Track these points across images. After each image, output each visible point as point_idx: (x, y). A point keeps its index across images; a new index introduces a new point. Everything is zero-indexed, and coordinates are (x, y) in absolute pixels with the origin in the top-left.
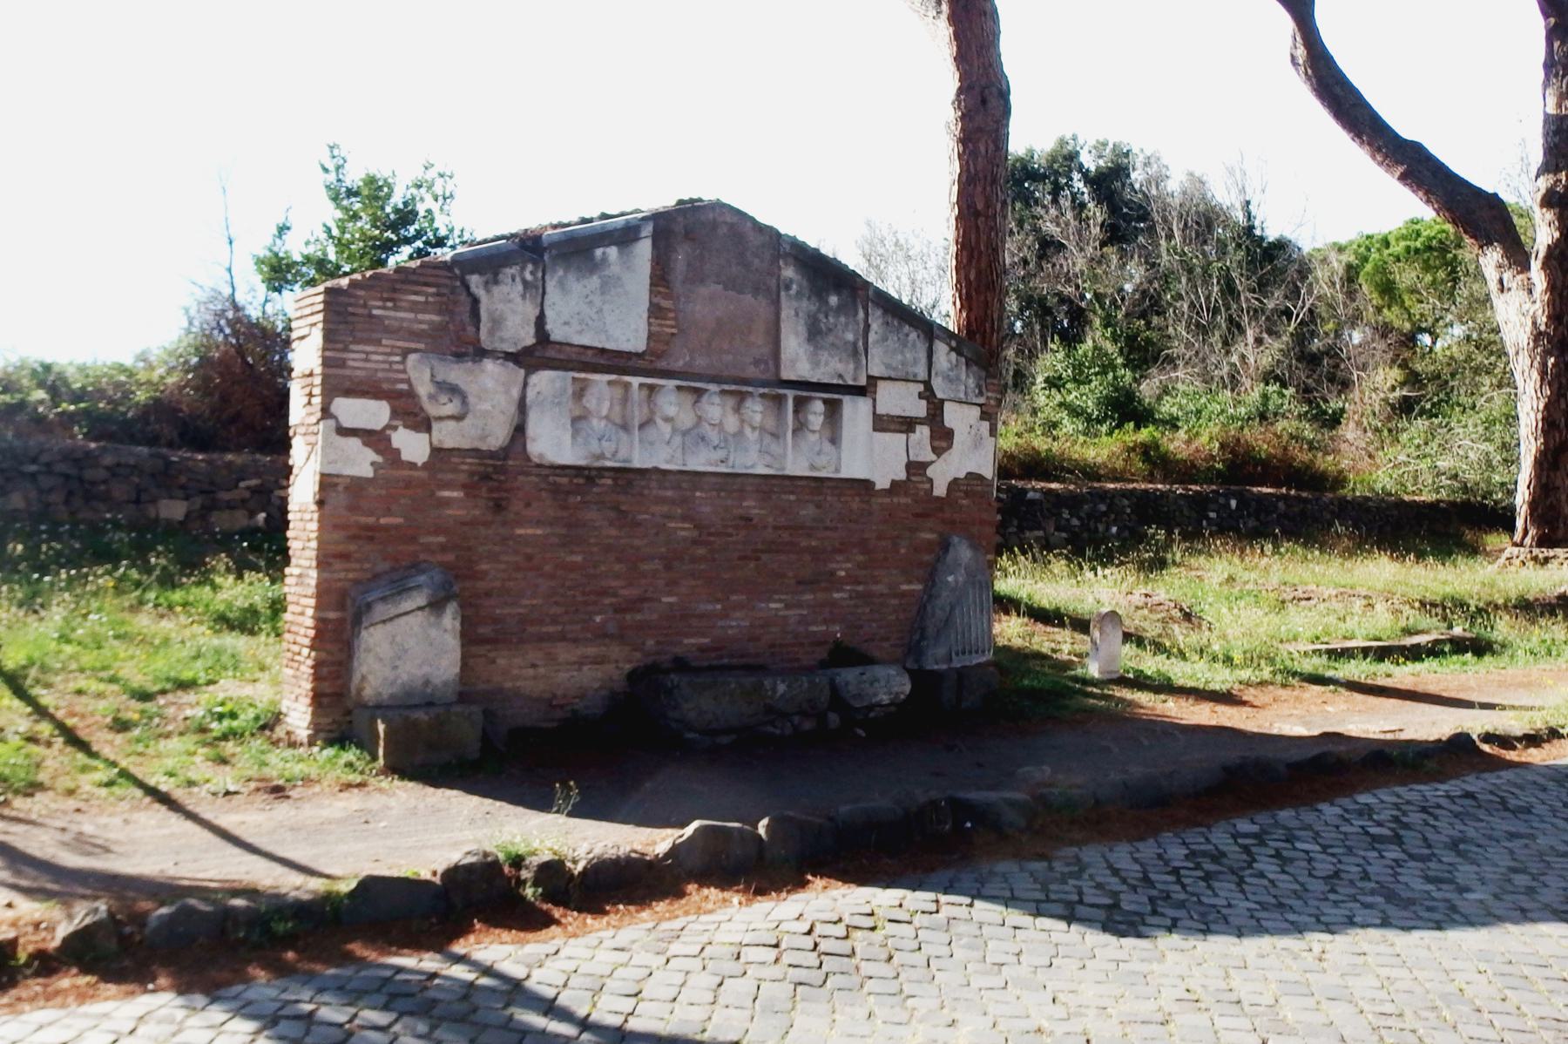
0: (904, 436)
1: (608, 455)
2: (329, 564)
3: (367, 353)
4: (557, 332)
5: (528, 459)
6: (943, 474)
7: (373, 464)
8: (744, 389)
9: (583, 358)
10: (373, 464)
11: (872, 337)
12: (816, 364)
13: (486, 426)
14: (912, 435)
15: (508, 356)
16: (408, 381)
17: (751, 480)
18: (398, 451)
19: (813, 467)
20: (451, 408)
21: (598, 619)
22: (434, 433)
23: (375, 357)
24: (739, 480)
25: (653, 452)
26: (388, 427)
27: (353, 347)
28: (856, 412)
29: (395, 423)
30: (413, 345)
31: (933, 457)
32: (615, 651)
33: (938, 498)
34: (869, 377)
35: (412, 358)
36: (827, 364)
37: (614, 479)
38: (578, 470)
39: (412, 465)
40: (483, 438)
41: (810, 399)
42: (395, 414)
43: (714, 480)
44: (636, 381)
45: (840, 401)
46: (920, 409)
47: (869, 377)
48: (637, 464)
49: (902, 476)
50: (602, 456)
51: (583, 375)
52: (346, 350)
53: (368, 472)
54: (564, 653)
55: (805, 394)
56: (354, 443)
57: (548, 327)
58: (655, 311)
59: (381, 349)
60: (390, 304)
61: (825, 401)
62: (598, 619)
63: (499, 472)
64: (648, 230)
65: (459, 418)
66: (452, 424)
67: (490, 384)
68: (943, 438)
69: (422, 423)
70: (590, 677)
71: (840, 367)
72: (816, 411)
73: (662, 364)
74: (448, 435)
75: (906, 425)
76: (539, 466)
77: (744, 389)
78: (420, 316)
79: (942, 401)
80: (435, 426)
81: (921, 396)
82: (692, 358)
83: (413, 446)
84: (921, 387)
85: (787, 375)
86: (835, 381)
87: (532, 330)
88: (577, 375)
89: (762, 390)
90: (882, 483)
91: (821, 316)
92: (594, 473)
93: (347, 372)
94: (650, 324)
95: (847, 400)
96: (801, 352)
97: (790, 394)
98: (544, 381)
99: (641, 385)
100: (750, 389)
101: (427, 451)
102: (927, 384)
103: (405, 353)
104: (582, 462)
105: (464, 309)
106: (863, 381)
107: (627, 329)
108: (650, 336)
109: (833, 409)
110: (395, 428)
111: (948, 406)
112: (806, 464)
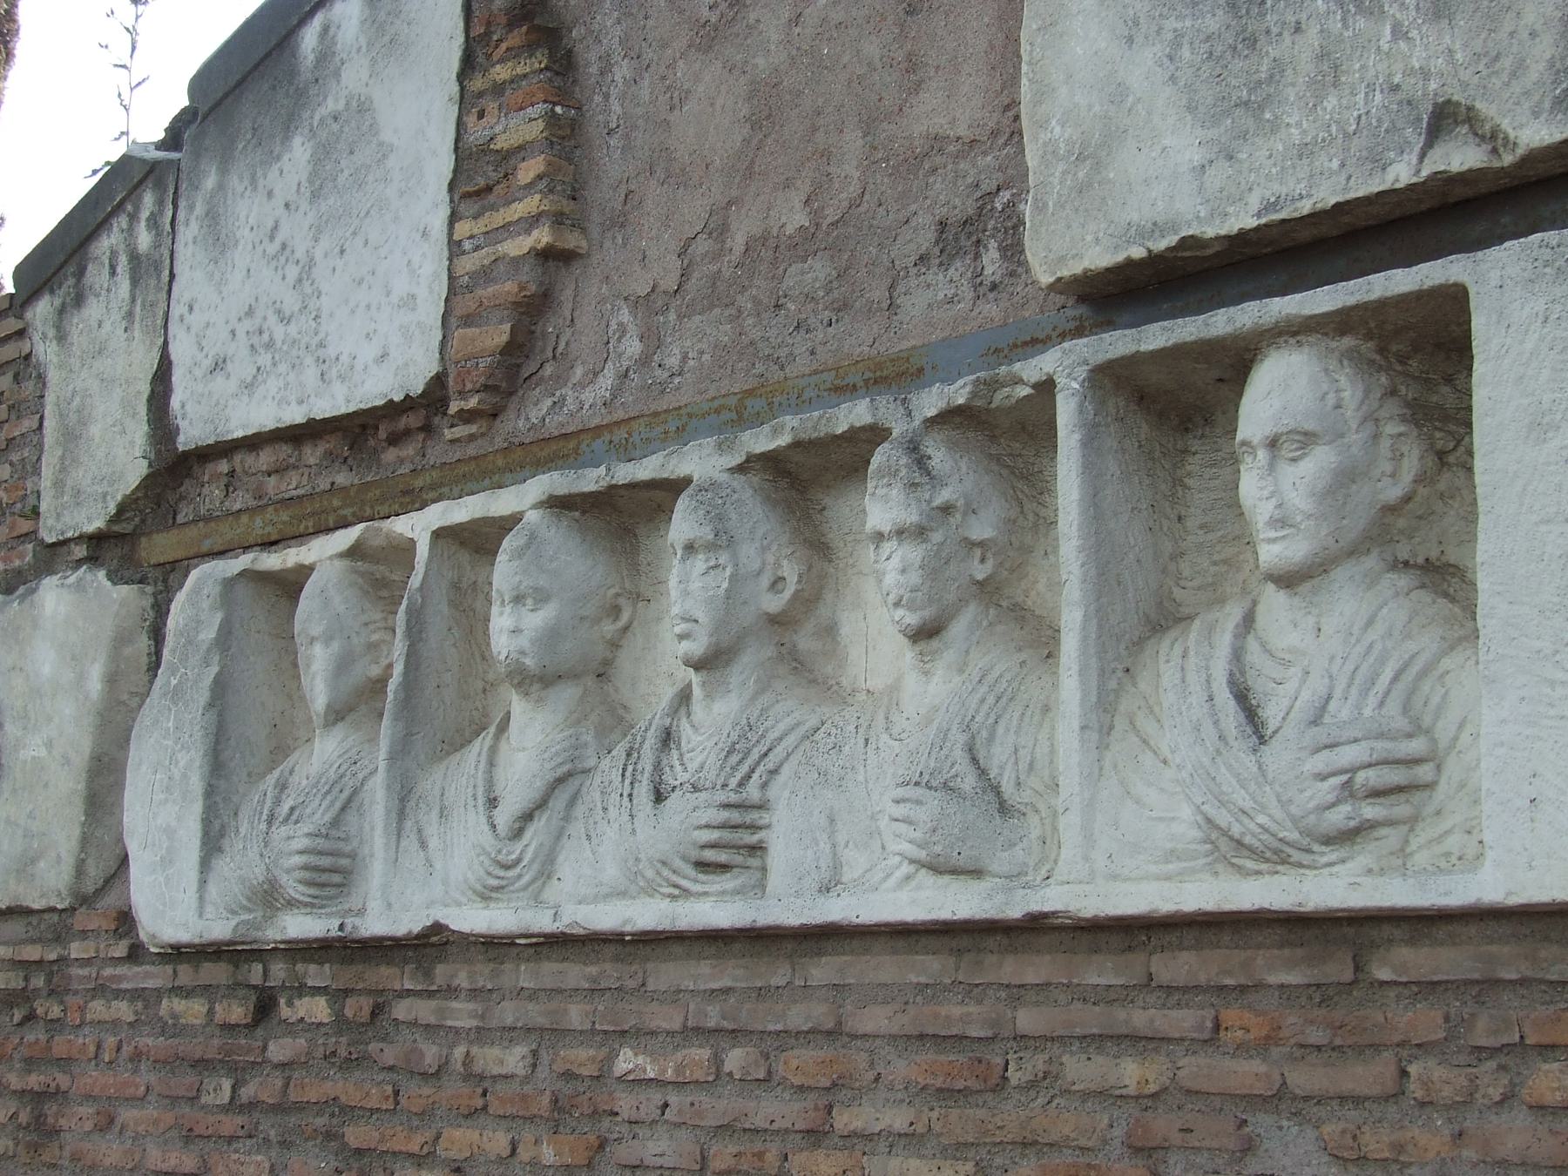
9: (293, 484)
12: (1242, 108)
17: (885, 968)
24: (823, 970)
36: (1330, 70)
37: (338, 996)
41: (1235, 362)
43: (703, 974)
45: (1455, 300)
55: (1156, 336)
71: (1434, 58)
82: (653, 340)
86: (1402, 173)
96: (1142, 69)
104: (219, 929)
109: (1426, 359)
112: (1184, 827)
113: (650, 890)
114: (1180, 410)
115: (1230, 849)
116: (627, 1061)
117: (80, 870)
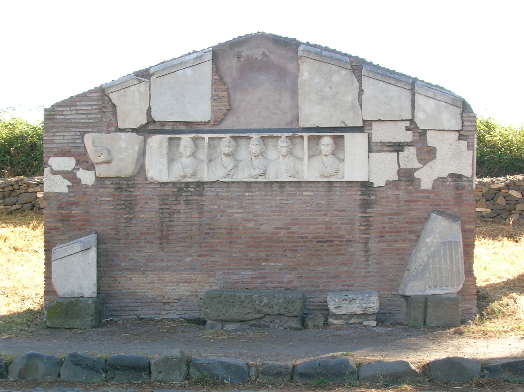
0: (396, 154)
1: (189, 176)
2: (49, 233)
3: (64, 136)
4: (157, 116)
5: (146, 179)
6: (427, 177)
7: (69, 186)
8: (275, 134)
10: (69, 186)
11: (364, 97)
13: (123, 165)
14: (401, 154)
15: (133, 130)
16: (85, 148)
18: (80, 180)
19: (323, 176)
20: (102, 159)
21: (188, 260)
22: (96, 171)
23: (67, 138)
25: (213, 173)
26: (74, 169)
27: (57, 134)
28: (355, 143)
29: (78, 167)
30: (86, 130)
31: (420, 166)
32: (199, 277)
33: (425, 191)
34: (364, 121)
35: (87, 136)
38: (174, 183)
39: (87, 186)
40: (120, 171)
42: (78, 162)
44: (207, 136)
45: (342, 137)
46: (408, 137)
47: (364, 121)
48: (206, 180)
49: (396, 178)
50: (185, 177)
51: (177, 136)
52: (54, 135)
53: (66, 190)
54: (167, 276)
56: (59, 177)
57: (153, 114)
58: (215, 99)
59: (71, 134)
60: (74, 112)
61: (335, 138)
62: (188, 260)
63: (125, 188)
64: (210, 56)
65: (108, 162)
66: (105, 166)
67: (123, 145)
68: (427, 154)
69: (90, 167)
70: (184, 290)
72: (326, 142)
73: (222, 126)
74: (102, 171)
75: (398, 147)
76: (151, 183)
77: (275, 134)
78: (89, 116)
79: (425, 131)
80: (97, 167)
81: (407, 129)
83: (87, 177)
84: (408, 124)
85: (303, 124)
87: (145, 116)
88: (173, 136)
89: (287, 134)
90: (378, 182)
91: (327, 89)
92: (183, 185)
93: (55, 146)
94: (213, 106)
95: (347, 136)
97: (306, 135)
98: (157, 142)
99: (209, 138)
100: (278, 134)
101: (94, 178)
102: (412, 121)
103: (83, 134)
105: (109, 111)
106: (360, 124)
107: (201, 111)
108: (213, 112)
110: (78, 169)
111: (429, 134)
112: (318, 174)
113: (253, 178)
114: (314, 141)
115: (323, 176)
116: (247, 194)
117: (133, 173)
